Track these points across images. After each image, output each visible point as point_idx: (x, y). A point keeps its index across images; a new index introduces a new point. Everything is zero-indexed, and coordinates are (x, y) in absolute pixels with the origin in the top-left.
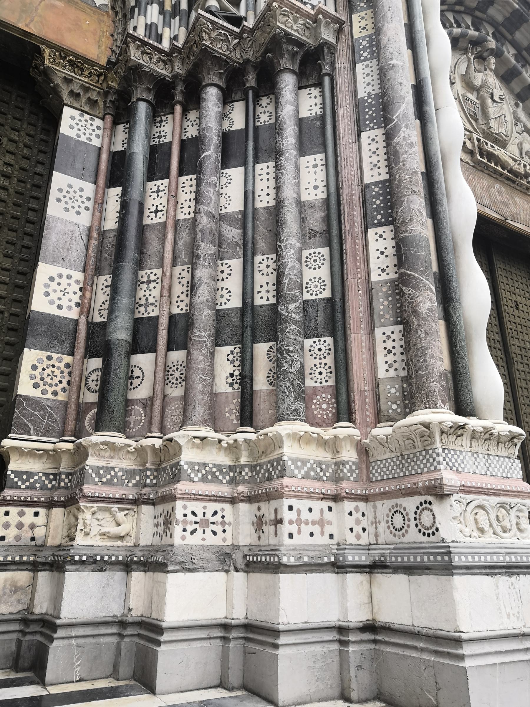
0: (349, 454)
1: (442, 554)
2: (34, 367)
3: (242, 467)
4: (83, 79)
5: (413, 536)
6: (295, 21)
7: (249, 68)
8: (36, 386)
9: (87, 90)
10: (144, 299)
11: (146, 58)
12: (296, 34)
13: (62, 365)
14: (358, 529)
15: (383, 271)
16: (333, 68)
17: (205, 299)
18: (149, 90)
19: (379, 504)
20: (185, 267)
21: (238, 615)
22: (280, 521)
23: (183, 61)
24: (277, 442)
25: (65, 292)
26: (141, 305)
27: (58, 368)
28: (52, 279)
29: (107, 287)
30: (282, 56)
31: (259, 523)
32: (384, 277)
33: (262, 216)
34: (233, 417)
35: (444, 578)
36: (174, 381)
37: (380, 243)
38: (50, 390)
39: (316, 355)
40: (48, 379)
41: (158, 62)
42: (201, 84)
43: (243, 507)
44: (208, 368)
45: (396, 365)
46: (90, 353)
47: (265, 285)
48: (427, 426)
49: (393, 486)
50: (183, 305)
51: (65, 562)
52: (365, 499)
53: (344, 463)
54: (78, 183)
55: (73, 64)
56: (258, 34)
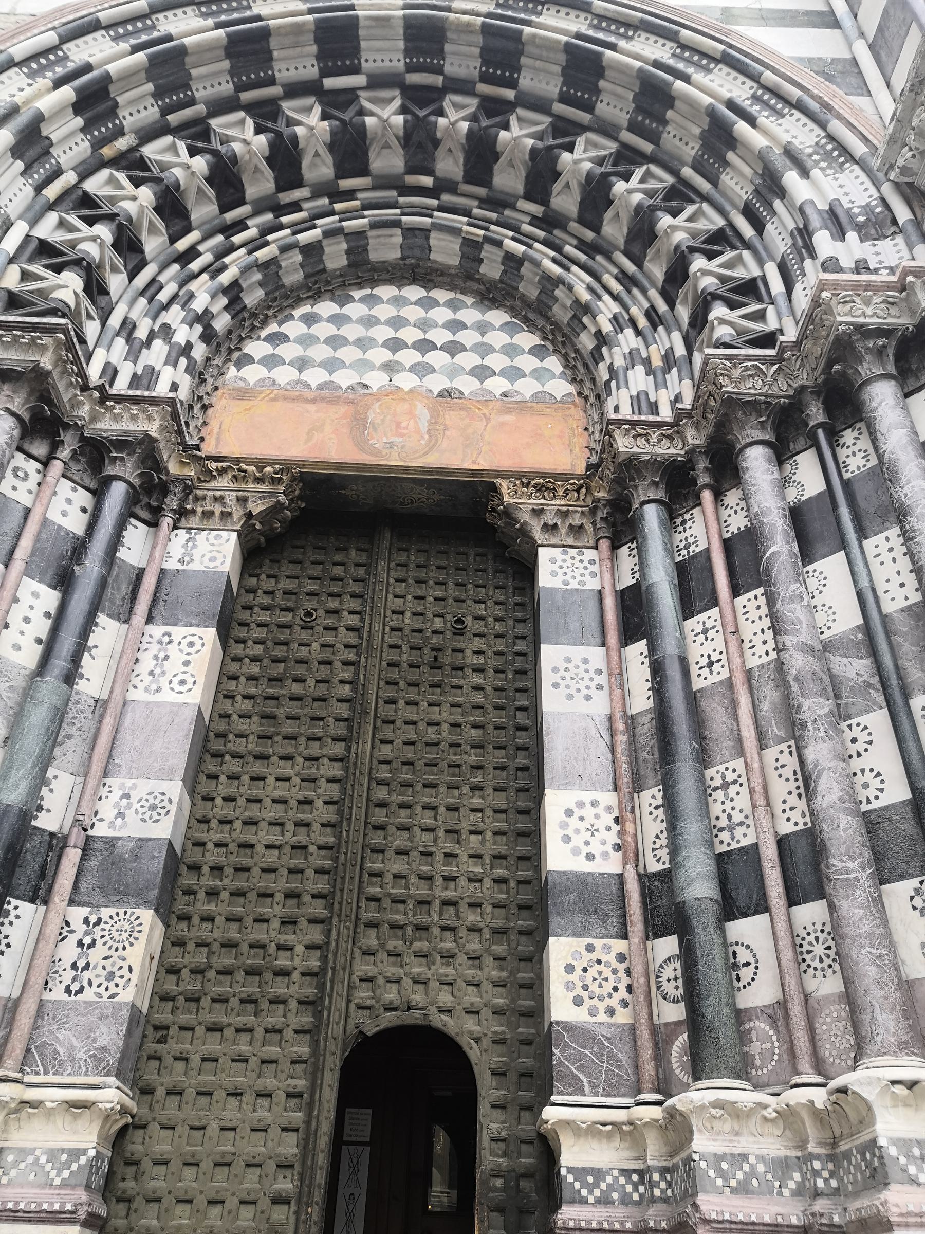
2: (570, 969)
4: (557, 502)
6: (867, 302)
7: (807, 397)
8: (578, 1001)
9: (565, 515)
10: (724, 817)
11: (641, 441)
13: (611, 958)
17: (835, 798)
18: (656, 484)
23: (697, 425)
25: (593, 831)
26: (721, 830)
27: (608, 965)
28: (569, 813)
29: (657, 807)
30: (860, 360)
33: (903, 625)
36: (816, 963)
38: (602, 1006)
40: (594, 987)
41: (660, 440)
42: (734, 447)
44: (878, 931)
46: (654, 930)
50: (796, 816)
54: (577, 652)
55: (540, 488)
56: (808, 345)
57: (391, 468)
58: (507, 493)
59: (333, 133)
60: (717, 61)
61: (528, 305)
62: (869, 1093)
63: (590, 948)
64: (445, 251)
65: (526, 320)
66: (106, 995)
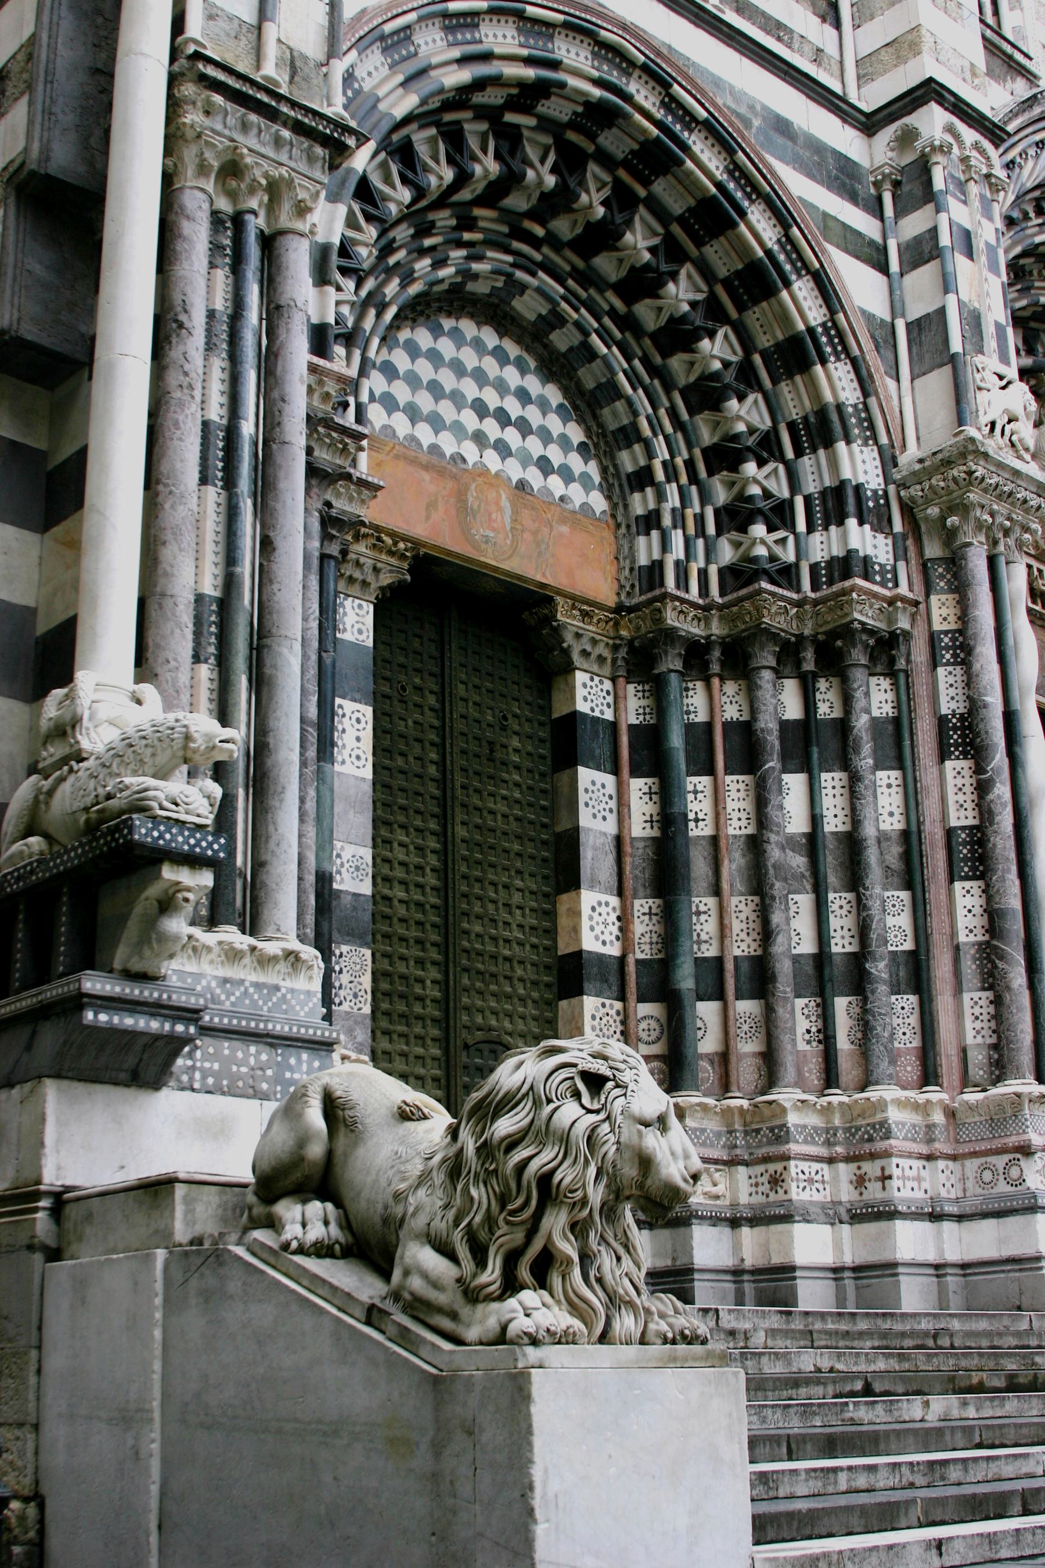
0: (938, 1117)
1: (1029, 1199)
2: (593, 1017)
3: (836, 1129)
4: (591, 628)
5: (1003, 1187)
12: (871, 622)
13: (613, 1012)
14: (948, 1185)
15: (971, 931)
16: (908, 661)
19: (968, 1163)
20: (742, 898)
21: (848, 1260)
22: (890, 1177)
23: (721, 618)
24: (881, 1105)
28: (593, 909)
29: (644, 914)
31: (860, 1181)
32: (972, 938)
33: (831, 844)
34: (814, 1077)
35: (1029, 1217)
37: (967, 898)
39: (900, 1013)
40: (605, 1030)
43: (842, 1166)
45: (983, 1032)
47: (839, 929)
48: (1018, 1095)
49: (984, 1146)
50: (744, 946)
51: (691, 1216)
52: (954, 1158)
53: (934, 1125)
55: (585, 614)
57: (487, 566)
58: (566, 617)
59: (499, 178)
60: (809, 272)
61: (580, 391)
62: (787, 1105)
63: (604, 1005)
64: (528, 307)
65: (576, 408)
66: (356, 1008)
